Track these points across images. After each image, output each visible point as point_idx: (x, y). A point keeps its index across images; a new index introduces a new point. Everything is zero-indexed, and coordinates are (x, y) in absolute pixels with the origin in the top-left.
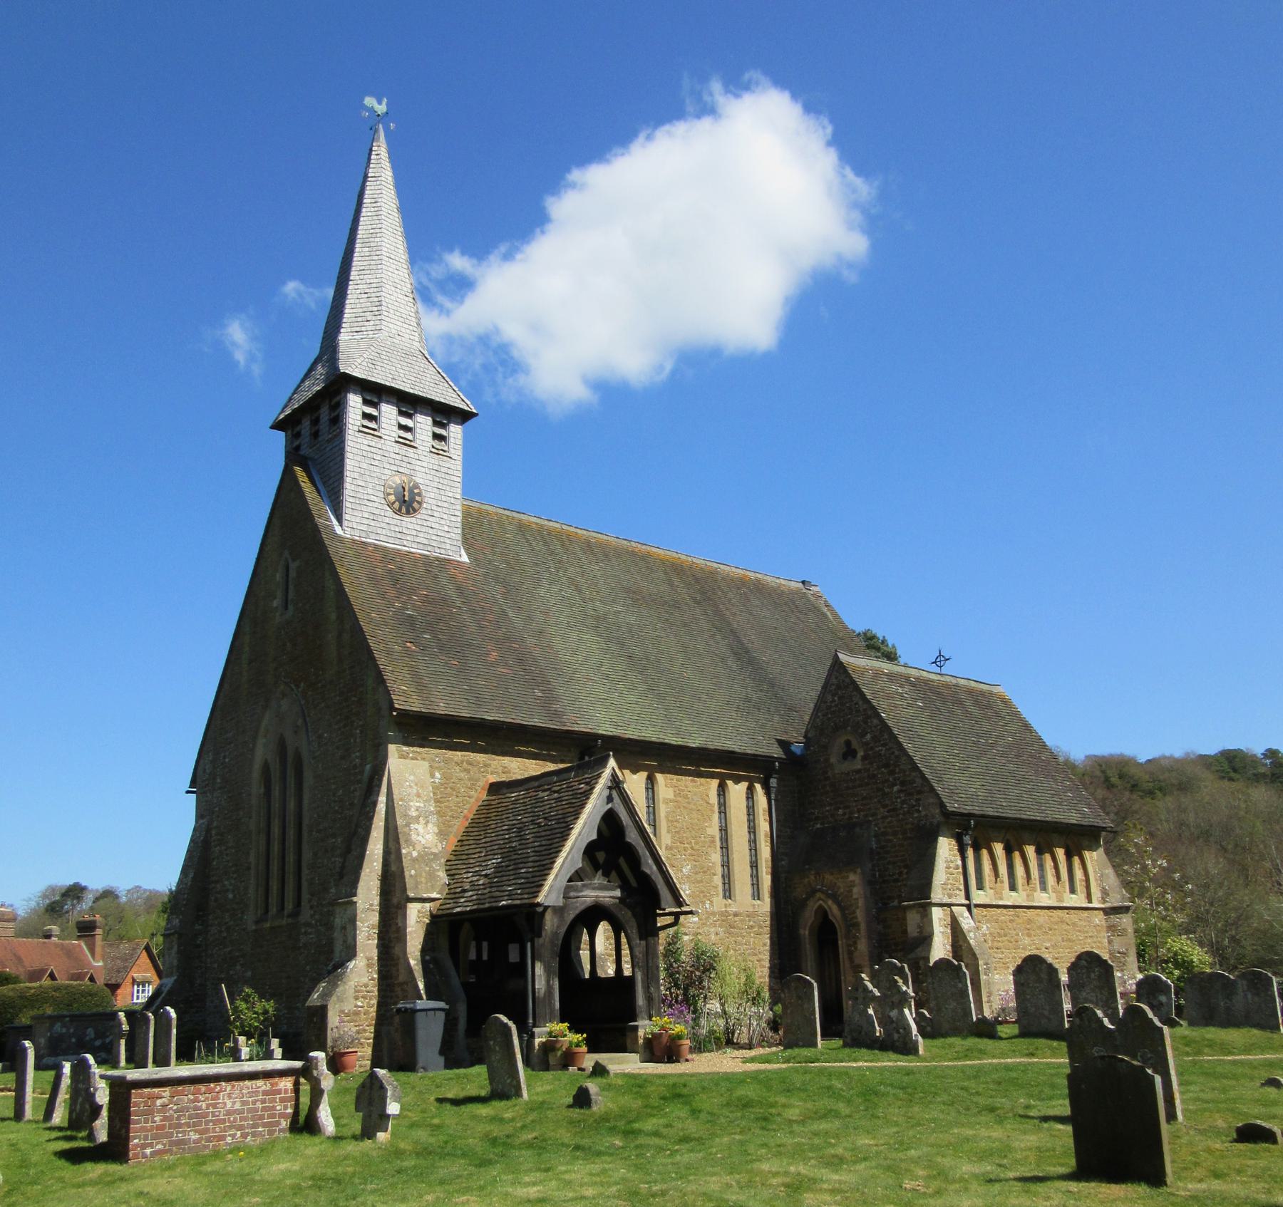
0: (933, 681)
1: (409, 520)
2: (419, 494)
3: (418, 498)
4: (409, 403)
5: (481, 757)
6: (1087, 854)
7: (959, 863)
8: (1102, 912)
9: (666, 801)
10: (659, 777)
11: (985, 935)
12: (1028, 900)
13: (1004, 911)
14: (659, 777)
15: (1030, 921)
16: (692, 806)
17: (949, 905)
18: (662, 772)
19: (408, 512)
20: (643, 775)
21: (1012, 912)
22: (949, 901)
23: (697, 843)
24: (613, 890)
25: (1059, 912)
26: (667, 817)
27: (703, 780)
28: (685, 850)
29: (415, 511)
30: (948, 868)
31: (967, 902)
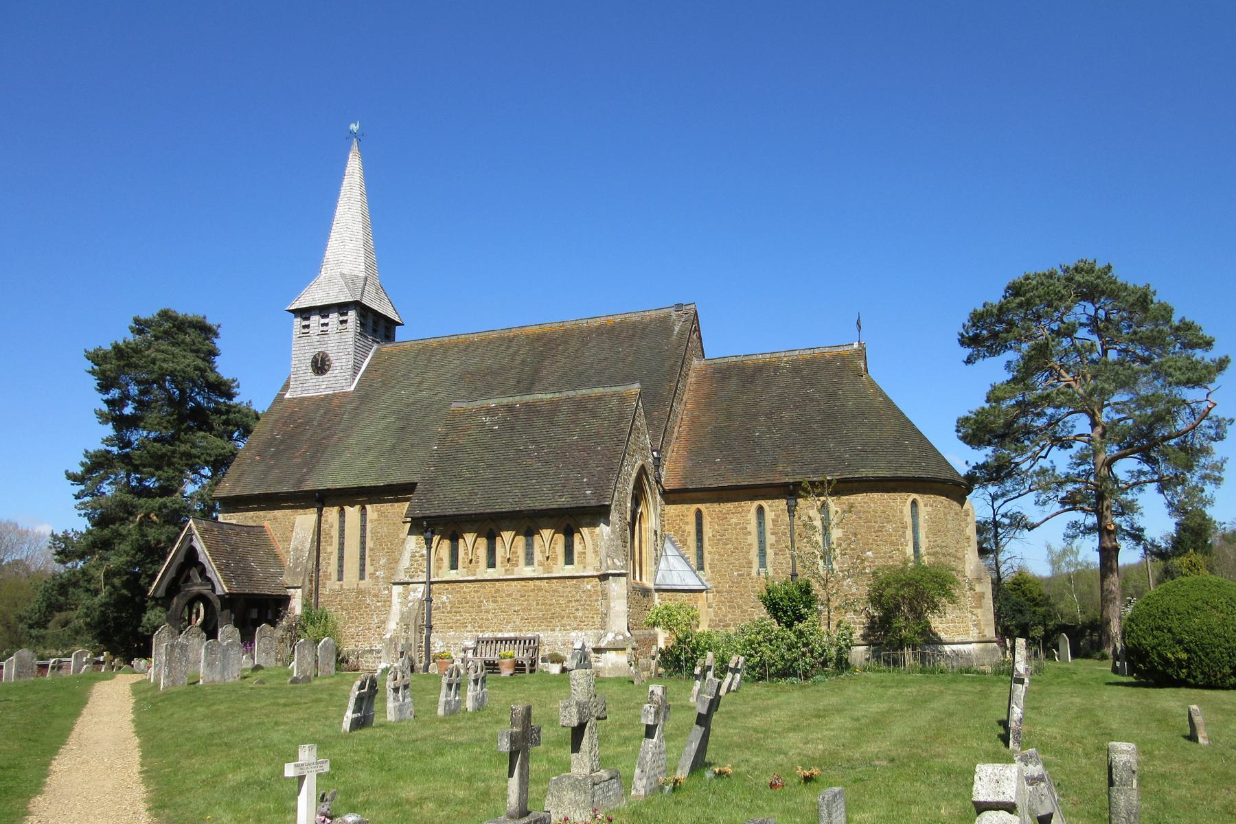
0: (542, 401)
1: (326, 376)
2: (328, 360)
3: (327, 363)
4: (324, 310)
5: (262, 513)
6: (585, 531)
7: (425, 552)
8: (597, 579)
9: (371, 521)
10: (368, 507)
11: (445, 603)
12: (506, 574)
13: (469, 585)
14: (368, 507)
15: (497, 591)
16: (390, 522)
17: (408, 583)
18: (370, 504)
19: (323, 373)
20: (358, 507)
21: (478, 585)
22: (406, 580)
23: (392, 544)
24: (207, 585)
25: (537, 582)
26: (371, 531)
27: (399, 504)
28: (383, 549)
29: (326, 371)
30: (413, 556)
31: (425, 580)
